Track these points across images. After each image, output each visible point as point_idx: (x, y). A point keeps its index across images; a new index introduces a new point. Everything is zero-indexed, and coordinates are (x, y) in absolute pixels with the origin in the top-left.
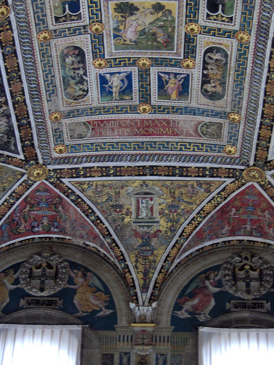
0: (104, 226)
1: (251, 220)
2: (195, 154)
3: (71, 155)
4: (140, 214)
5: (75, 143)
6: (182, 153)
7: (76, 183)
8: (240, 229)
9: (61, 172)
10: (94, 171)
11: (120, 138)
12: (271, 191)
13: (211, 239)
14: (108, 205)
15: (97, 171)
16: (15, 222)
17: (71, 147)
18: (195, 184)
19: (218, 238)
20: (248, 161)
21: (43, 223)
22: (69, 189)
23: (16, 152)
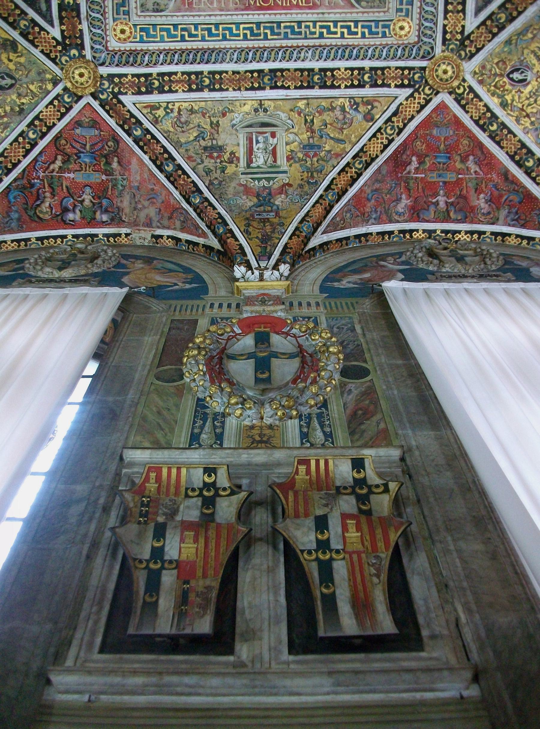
0: (189, 180)
1: (445, 183)
2: (344, 44)
3: (139, 46)
4: (254, 160)
5: (148, 20)
6: (323, 42)
7: (145, 107)
8: (428, 204)
9: (120, 82)
10: (177, 81)
11: (221, 15)
12: (476, 105)
13: (379, 221)
14: (197, 147)
15: (182, 81)
16: (34, 190)
17: (142, 30)
18: (347, 104)
19: (391, 222)
20: (432, 48)
21: (82, 202)
22: (132, 116)
23: (48, 17)
